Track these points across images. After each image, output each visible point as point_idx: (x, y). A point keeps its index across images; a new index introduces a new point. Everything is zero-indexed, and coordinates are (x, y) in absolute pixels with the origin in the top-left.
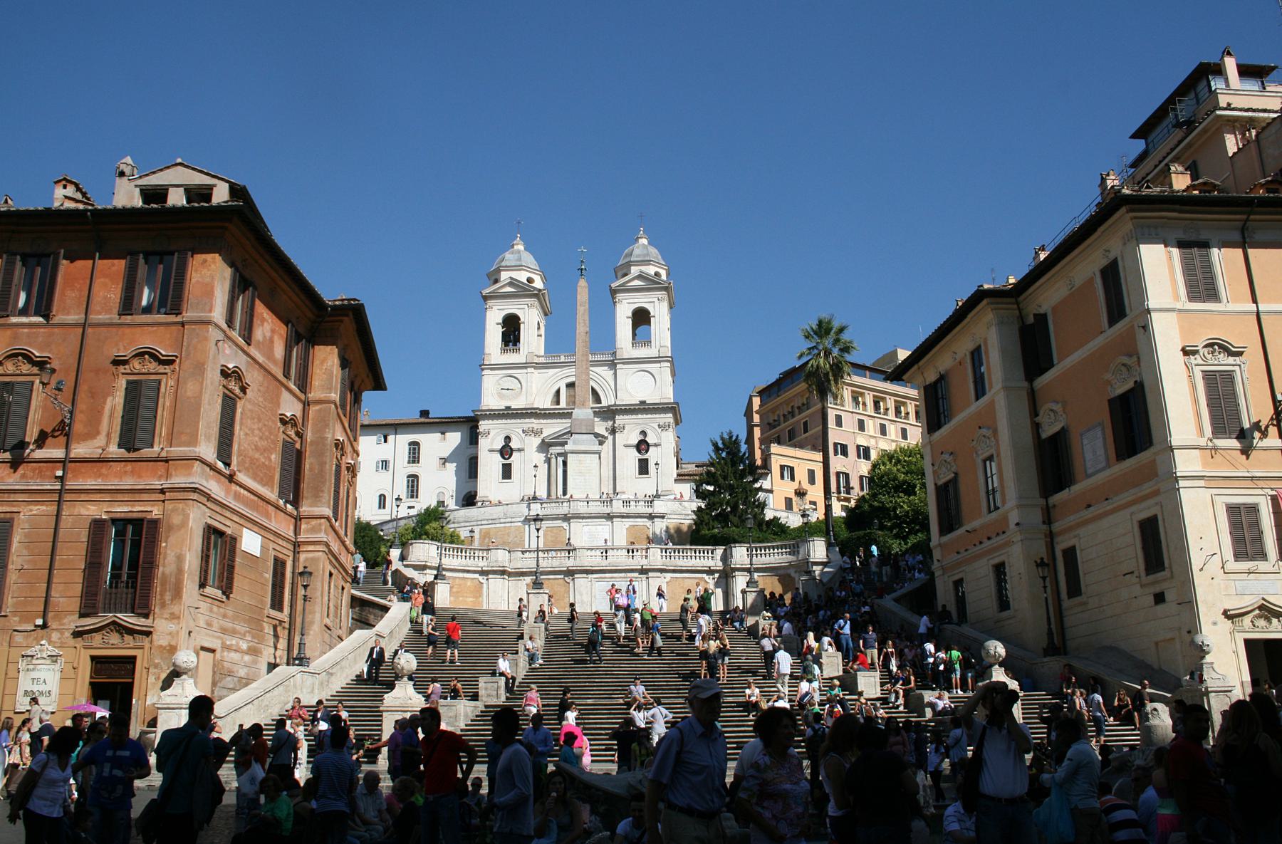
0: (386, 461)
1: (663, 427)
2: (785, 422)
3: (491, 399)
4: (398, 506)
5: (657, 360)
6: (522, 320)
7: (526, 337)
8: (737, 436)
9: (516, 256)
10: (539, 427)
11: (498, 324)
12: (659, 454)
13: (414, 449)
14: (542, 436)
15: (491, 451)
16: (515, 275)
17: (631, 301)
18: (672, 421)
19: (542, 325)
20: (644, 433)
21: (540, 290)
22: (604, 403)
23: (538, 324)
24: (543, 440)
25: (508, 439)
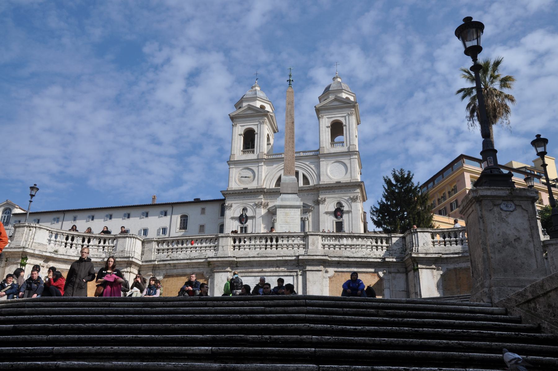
0: (165, 229)
1: (354, 200)
2: (439, 204)
3: (235, 185)
4: (32, 196)
5: (350, 153)
6: (256, 131)
7: (259, 142)
8: (409, 172)
9: (253, 93)
10: (266, 201)
11: (240, 135)
12: (350, 218)
13: (184, 220)
14: (268, 207)
15: (233, 218)
16: (252, 103)
17: (330, 116)
18: (360, 195)
19: (271, 138)
20: (339, 204)
21: (268, 112)
22: (311, 184)
23: (268, 135)
24: (269, 210)
25: (245, 209)
